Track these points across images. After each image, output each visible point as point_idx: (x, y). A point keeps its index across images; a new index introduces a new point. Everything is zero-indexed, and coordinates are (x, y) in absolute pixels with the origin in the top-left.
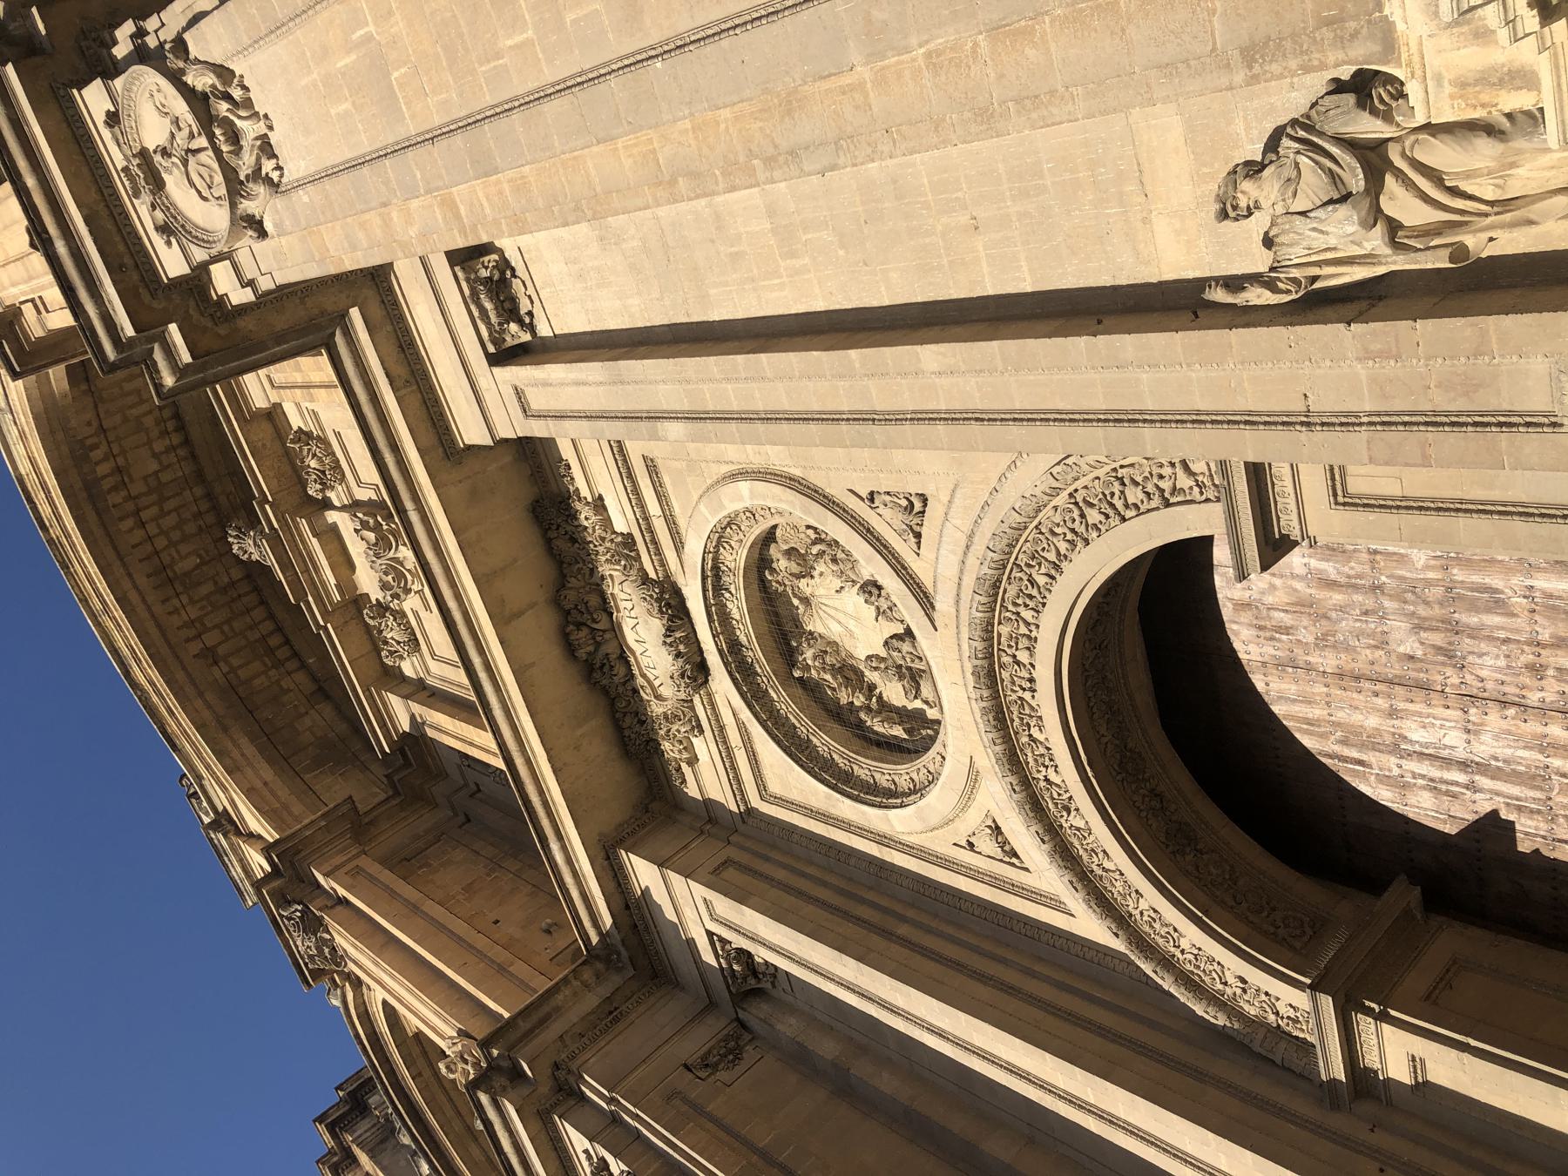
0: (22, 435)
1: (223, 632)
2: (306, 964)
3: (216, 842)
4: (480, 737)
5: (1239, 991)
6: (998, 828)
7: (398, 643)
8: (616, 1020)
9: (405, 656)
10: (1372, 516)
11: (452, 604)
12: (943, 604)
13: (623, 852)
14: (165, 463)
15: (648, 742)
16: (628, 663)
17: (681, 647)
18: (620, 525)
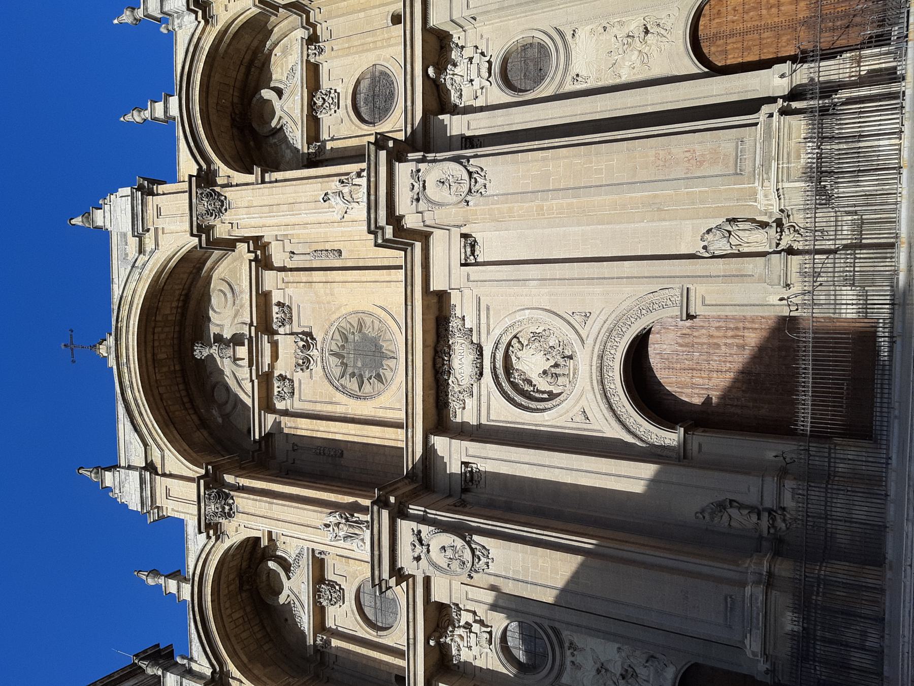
0: (139, 280)
1: (166, 388)
2: (205, 520)
3: (143, 476)
4: (328, 426)
5: (655, 440)
6: (584, 412)
7: (285, 393)
8: (417, 496)
9: (286, 399)
10: (710, 307)
11: (409, 338)
12: (589, 342)
13: (433, 436)
14: (173, 312)
15: (445, 403)
16: (450, 373)
17: (478, 365)
18: (468, 325)
